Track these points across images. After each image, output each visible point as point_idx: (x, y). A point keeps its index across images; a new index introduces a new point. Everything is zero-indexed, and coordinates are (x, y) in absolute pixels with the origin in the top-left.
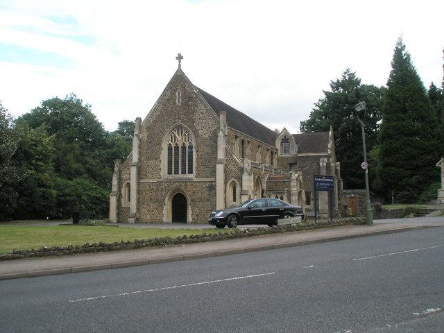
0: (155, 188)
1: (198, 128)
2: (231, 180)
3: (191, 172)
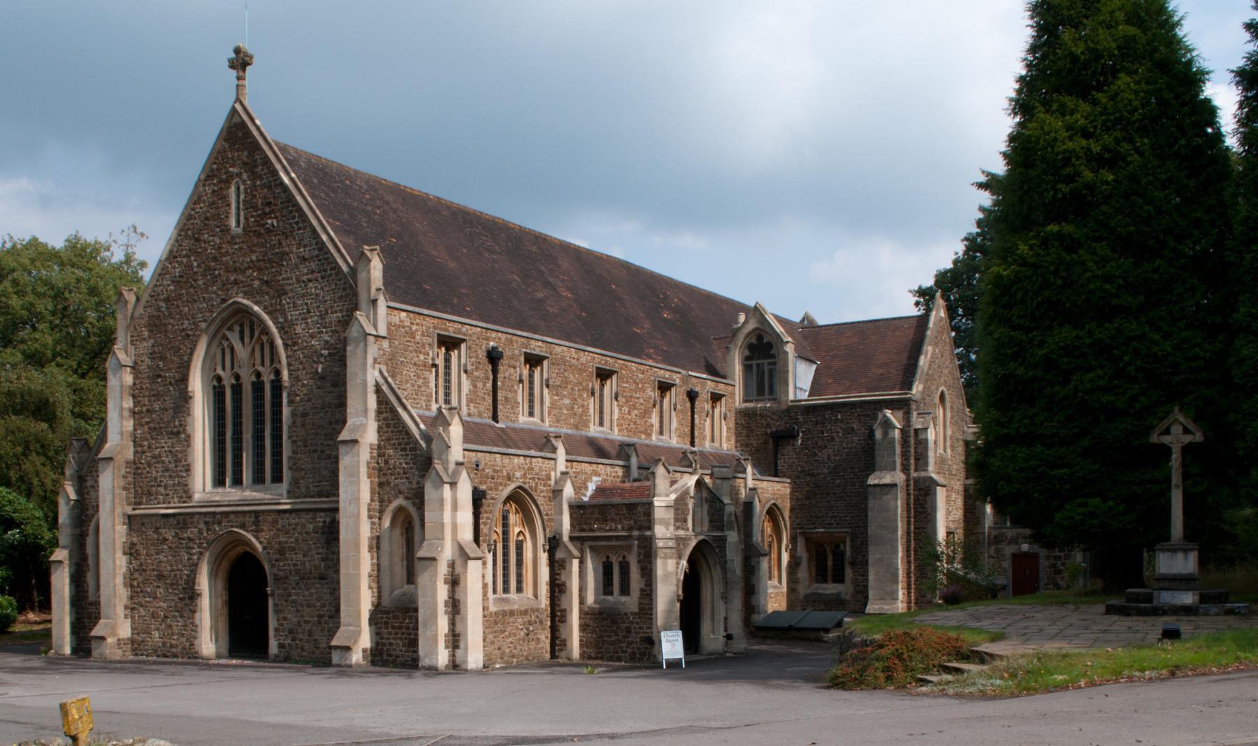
1: (292, 314)
2: (395, 504)
3: (277, 478)
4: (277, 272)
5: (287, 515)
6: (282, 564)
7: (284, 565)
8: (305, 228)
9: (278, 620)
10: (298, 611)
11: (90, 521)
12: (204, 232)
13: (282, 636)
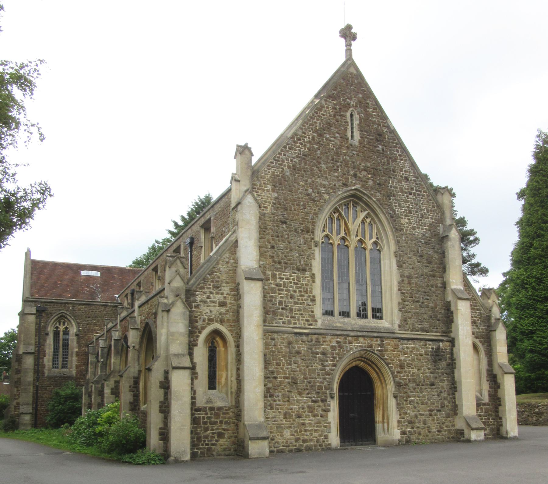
0: (304, 349)
1: (399, 211)
4: (386, 180)
5: (405, 342)
6: (402, 375)
7: (404, 376)
8: (405, 160)
9: (400, 415)
10: (415, 407)
11: (200, 333)
12: (325, 131)
13: (404, 426)
